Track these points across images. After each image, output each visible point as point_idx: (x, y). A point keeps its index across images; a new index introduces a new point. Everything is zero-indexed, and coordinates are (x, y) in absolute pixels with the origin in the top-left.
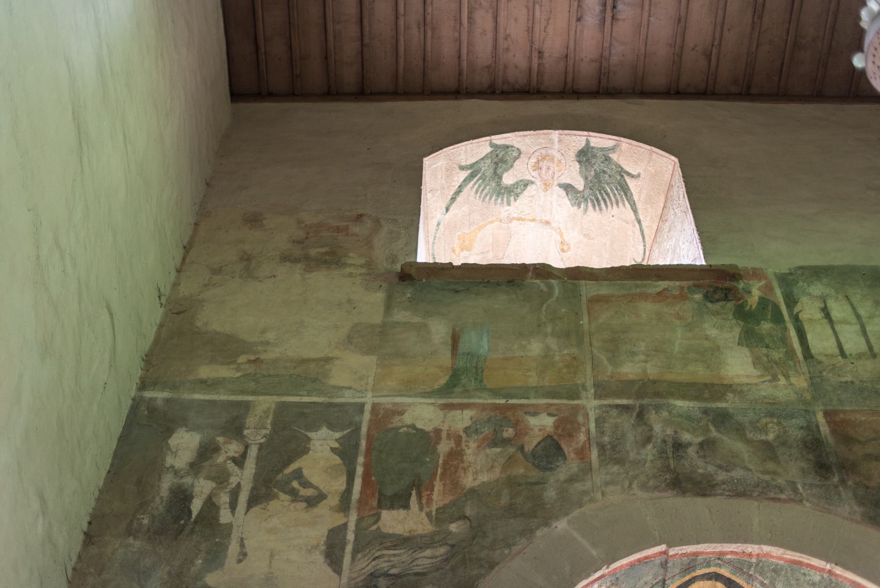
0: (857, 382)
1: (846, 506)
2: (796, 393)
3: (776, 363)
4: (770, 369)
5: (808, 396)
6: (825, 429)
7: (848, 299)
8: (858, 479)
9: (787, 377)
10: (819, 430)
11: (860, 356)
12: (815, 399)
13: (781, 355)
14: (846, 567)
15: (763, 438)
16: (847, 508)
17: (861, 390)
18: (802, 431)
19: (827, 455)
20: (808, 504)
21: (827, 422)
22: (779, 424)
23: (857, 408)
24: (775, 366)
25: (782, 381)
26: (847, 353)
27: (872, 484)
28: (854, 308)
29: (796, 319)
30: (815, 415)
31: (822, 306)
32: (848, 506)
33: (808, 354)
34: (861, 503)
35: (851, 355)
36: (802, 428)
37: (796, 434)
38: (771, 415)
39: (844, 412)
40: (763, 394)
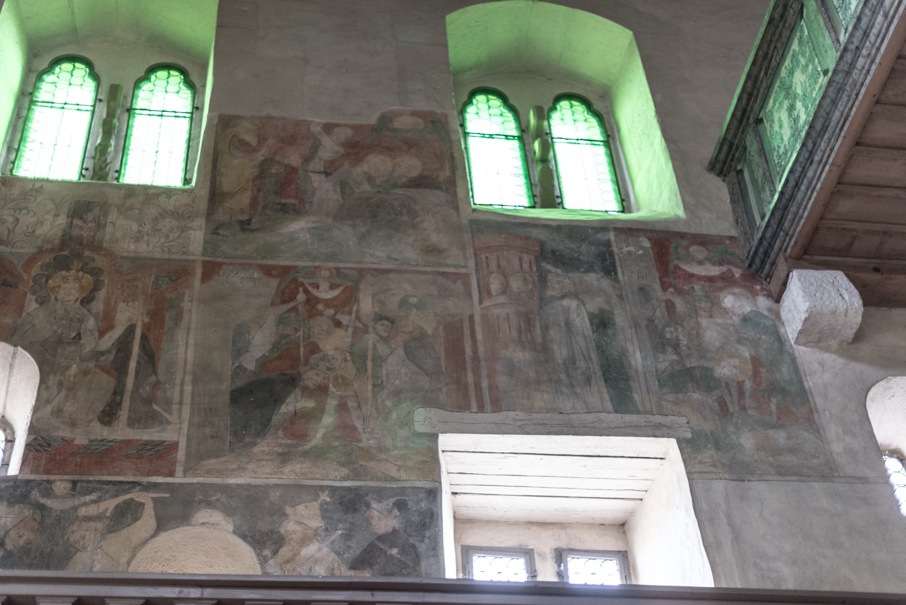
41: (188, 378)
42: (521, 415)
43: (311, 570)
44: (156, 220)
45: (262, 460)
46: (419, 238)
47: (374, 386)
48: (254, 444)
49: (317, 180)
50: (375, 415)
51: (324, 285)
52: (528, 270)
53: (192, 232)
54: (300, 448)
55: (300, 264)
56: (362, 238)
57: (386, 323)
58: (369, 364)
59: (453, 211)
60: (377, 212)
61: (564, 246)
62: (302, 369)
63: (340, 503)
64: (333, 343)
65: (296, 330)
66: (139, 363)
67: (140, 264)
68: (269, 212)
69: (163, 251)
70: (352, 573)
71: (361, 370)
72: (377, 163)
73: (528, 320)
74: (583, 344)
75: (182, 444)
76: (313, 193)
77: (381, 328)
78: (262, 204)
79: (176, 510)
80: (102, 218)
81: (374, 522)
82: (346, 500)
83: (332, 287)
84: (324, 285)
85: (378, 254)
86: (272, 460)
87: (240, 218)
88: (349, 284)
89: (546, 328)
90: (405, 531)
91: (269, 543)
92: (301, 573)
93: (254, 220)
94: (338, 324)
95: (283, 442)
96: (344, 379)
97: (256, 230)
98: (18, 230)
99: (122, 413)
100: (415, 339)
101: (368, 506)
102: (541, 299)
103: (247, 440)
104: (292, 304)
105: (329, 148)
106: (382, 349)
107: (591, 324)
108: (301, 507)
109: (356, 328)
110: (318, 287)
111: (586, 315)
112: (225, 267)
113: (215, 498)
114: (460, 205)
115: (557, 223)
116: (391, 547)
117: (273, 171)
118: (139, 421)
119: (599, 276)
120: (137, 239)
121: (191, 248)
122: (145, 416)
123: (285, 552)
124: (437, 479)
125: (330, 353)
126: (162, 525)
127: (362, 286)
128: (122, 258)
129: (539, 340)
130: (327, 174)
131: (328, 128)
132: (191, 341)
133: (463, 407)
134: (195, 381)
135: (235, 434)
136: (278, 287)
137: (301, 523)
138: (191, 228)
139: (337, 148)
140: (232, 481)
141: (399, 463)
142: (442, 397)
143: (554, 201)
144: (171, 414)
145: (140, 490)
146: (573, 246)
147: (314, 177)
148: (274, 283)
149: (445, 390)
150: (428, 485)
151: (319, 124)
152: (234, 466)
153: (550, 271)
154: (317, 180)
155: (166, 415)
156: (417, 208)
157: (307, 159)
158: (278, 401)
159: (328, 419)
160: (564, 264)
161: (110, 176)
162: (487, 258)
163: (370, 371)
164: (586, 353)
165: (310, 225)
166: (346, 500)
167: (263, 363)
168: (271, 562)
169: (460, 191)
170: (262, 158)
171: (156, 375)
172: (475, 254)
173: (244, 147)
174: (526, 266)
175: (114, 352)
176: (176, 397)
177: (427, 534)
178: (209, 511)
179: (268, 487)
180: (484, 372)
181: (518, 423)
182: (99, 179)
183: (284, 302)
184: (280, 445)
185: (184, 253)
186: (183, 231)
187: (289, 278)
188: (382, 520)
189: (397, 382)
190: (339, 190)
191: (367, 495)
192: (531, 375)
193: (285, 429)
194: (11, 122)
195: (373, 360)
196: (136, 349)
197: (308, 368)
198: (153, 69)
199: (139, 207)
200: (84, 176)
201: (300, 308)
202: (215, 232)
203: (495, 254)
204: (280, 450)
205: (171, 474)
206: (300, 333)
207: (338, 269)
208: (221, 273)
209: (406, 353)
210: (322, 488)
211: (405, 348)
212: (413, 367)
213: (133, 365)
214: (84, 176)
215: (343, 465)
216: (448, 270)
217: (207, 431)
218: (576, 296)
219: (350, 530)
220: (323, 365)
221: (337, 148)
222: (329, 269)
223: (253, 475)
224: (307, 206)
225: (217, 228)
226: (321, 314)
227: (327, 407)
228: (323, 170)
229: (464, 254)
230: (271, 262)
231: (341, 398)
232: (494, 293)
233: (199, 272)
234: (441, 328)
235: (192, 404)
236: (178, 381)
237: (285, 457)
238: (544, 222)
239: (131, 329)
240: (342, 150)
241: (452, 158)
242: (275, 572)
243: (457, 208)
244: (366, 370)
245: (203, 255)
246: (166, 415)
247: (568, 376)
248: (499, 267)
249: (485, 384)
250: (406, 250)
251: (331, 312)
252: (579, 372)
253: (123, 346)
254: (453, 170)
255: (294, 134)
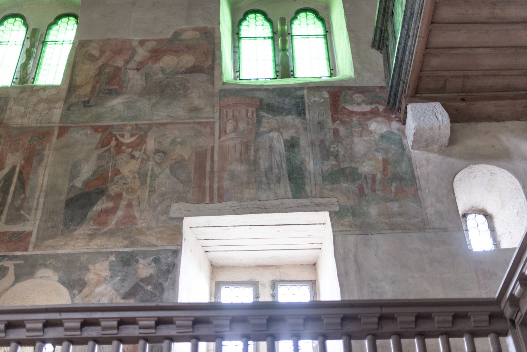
41: (43, 194)
42: (234, 203)
43: (99, 300)
44: (35, 105)
45: (78, 239)
46: (187, 103)
47: (150, 192)
48: (75, 230)
49: (131, 74)
50: (148, 208)
51: (127, 135)
52: (251, 117)
53: (55, 110)
54: (102, 231)
55: (116, 123)
56: (154, 105)
57: (161, 154)
58: (148, 179)
59: (210, 85)
60: (163, 90)
61: (275, 100)
62: (108, 185)
63: (121, 261)
64: (128, 168)
65: (108, 162)
66: (16, 187)
67: (23, 130)
68: (101, 95)
69: (37, 122)
70: (123, 301)
71: (143, 183)
72: (169, 61)
73: (247, 147)
74: (278, 158)
75: (35, 233)
76: (129, 82)
77: (157, 159)
78: (98, 90)
79: (27, 270)
80: (4, 106)
81: (139, 271)
82: (124, 259)
83: (132, 136)
84: (127, 135)
85: (161, 114)
86: (84, 239)
87: (83, 100)
88: (142, 133)
89: (257, 150)
90: (157, 276)
91: (78, 286)
92: (94, 302)
93: (92, 100)
94: (133, 157)
95: (93, 227)
96: (132, 188)
97: (92, 106)
99: (3, 217)
100: (177, 162)
101: (137, 262)
102: (257, 134)
103: (72, 227)
104: (107, 148)
105: (142, 53)
106: (157, 170)
107: (285, 146)
108: (98, 264)
109: (143, 159)
110: (123, 136)
111: (282, 141)
112: (71, 129)
113: (49, 262)
114: (215, 81)
115: (273, 87)
116: (148, 285)
117: (107, 71)
118: (12, 220)
119: (294, 117)
120: (23, 117)
121: (53, 120)
122: (16, 217)
123: (86, 291)
124: (180, 244)
125: (126, 174)
126: (18, 279)
127: (149, 134)
128: (14, 128)
129: (252, 158)
130: (138, 70)
131: (142, 43)
132: (47, 174)
133: (201, 200)
134: (46, 197)
135: (65, 225)
136: (101, 138)
137: (97, 274)
138: (54, 108)
139: (145, 54)
140: (60, 252)
141: (158, 236)
142: (189, 196)
143: (289, 74)
144: (30, 215)
145: (7, 260)
146: (280, 100)
147: (130, 72)
148: (99, 136)
149: (191, 191)
150: (173, 248)
151: (137, 40)
152: (62, 243)
153: (264, 116)
154: (131, 74)
155: (27, 216)
156: (189, 85)
157: (127, 62)
158: (92, 204)
159: (120, 213)
160: (273, 111)
161: (29, 81)
162: (227, 111)
163: (148, 183)
164: (279, 164)
165: (124, 101)
166: (124, 259)
167: (87, 183)
168: (77, 297)
169: (216, 73)
170: (101, 64)
171: (25, 194)
172: (220, 110)
173: (92, 58)
174: (250, 114)
175: (2, 183)
176: (35, 206)
177: (170, 276)
178: (45, 270)
179: (80, 254)
180: (216, 179)
181: (233, 208)
182: (22, 84)
183: (103, 146)
184: (91, 229)
185: (49, 122)
186: (50, 110)
187: (107, 133)
188: (145, 269)
189: (163, 189)
190: (144, 78)
191: (137, 255)
192: (244, 179)
193: (94, 220)
195: (151, 177)
196: (15, 180)
197: (112, 184)
198: (59, 17)
199: (26, 98)
200: (14, 83)
201: (112, 149)
202: (68, 109)
203: (232, 109)
204: (90, 232)
205: (26, 250)
206: (110, 164)
207: (137, 125)
208: (69, 133)
209: (171, 172)
210: (111, 253)
211: (170, 169)
212: (174, 180)
213: (12, 189)
214: (14, 83)
215: (125, 239)
216: (202, 120)
217: (50, 224)
218: (278, 130)
219: (125, 276)
220: (121, 182)
221: (145, 54)
222: (132, 126)
223: (73, 247)
224: (124, 89)
225: (70, 107)
226: (124, 152)
227: (120, 206)
228: (136, 67)
229: (213, 110)
230: (98, 124)
231: (129, 200)
232: (228, 132)
233: (56, 133)
234: (194, 155)
235: (43, 209)
236: (36, 196)
237: (92, 236)
238: (265, 87)
239: (13, 169)
240: (148, 55)
241: (214, 53)
242: (79, 302)
243: (213, 83)
244: (146, 183)
245: (60, 123)
246: (27, 216)
247: (267, 178)
248: (233, 116)
249: (216, 186)
250: (179, 110)
251: (130, 150)
252: (274, 175)
253: (8, 179)
254: (213, 61)
255: (122, 48)
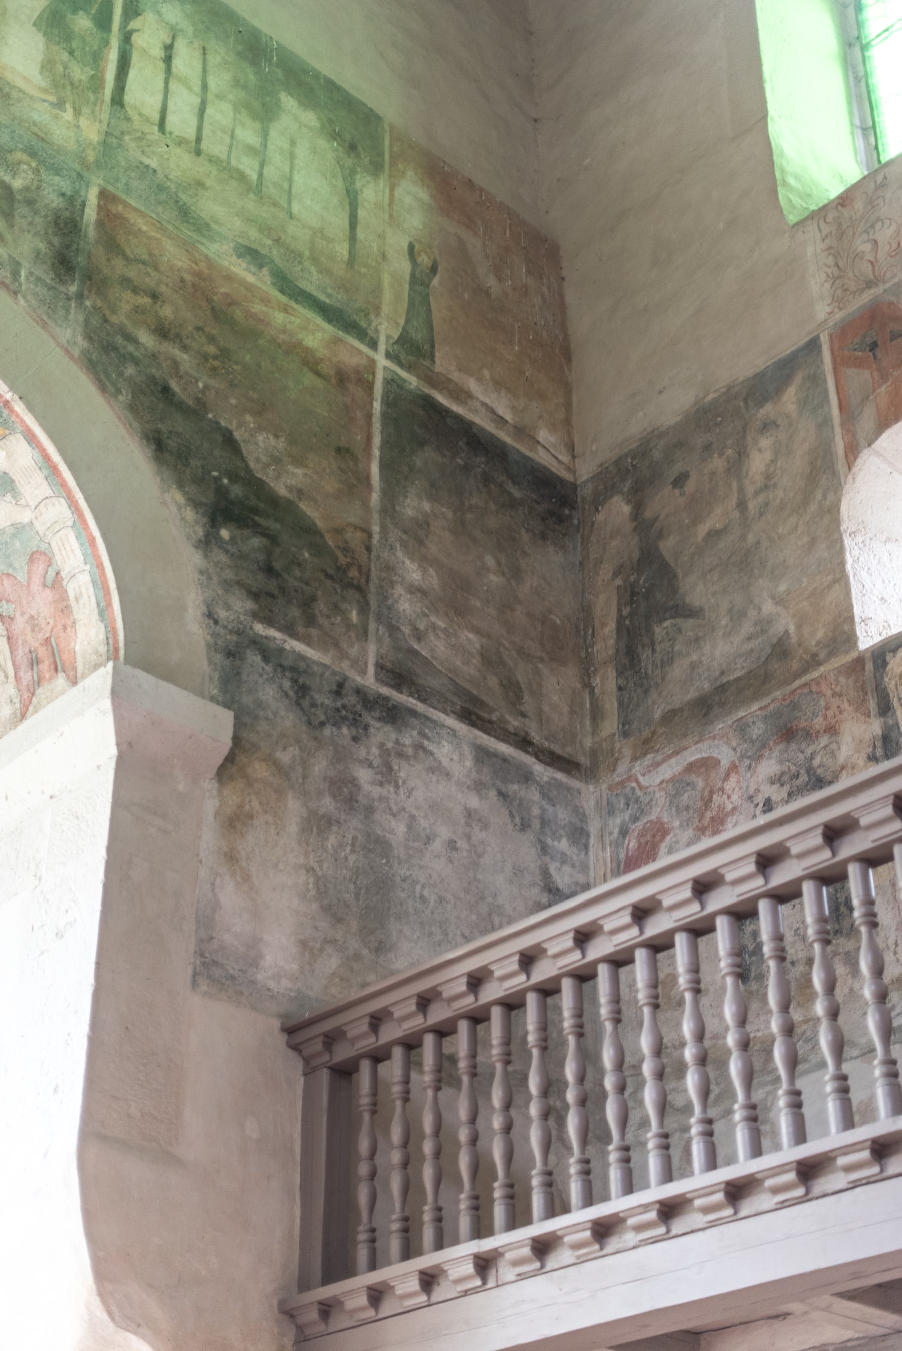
0: (160, 175)
1: (69, 330)
2: (78, 142)
3: (72, 84)
4: (61, 85)
5: (91, 156)
6: (91, 214)
7: (205, 54)
8: (99, 303)
9: (77, 113)
10: (83, 211)
11: (181, 142)
12: (98, 164)
13: (84, 77)
14: (30, 408)
15: (7, 179)
16: (68, 333)
17: (161, 188)
18: (61, 199)
19: (77, 250)
20: (22, 302)
21: (99, 206)
22: (36, 171)
23: (143, 209)
24: (68, 88)
25: (68, 115)
26: (168, 128)
27: (114, 319)
28: (205, 71)
29: (127, 38)
30: (88, 187)
31: (169, 41)
32: (71, 332)
33: (118, 100)
34: (89, 338)
35: (171, 133)
36: (63, 195)
37: (51, 199)
38: (33, 154)
39: (126, 205)
40: (35, 117)
98: (881, 255)
194: (849, 95)
